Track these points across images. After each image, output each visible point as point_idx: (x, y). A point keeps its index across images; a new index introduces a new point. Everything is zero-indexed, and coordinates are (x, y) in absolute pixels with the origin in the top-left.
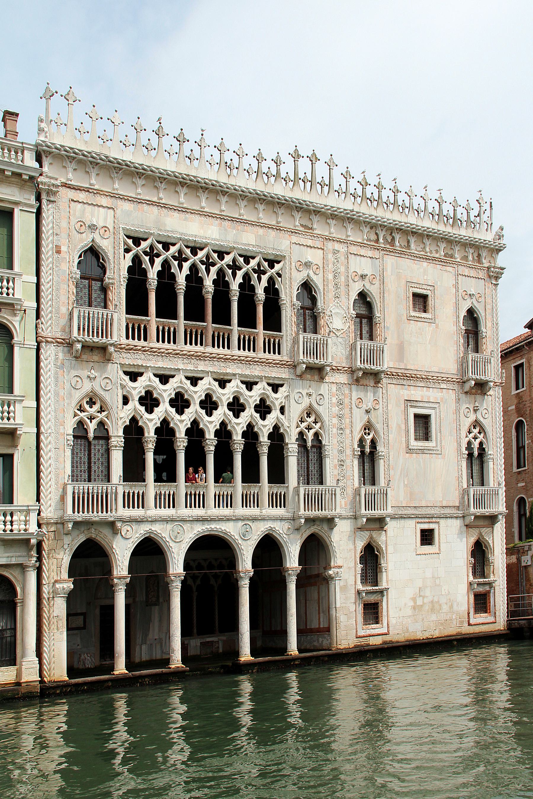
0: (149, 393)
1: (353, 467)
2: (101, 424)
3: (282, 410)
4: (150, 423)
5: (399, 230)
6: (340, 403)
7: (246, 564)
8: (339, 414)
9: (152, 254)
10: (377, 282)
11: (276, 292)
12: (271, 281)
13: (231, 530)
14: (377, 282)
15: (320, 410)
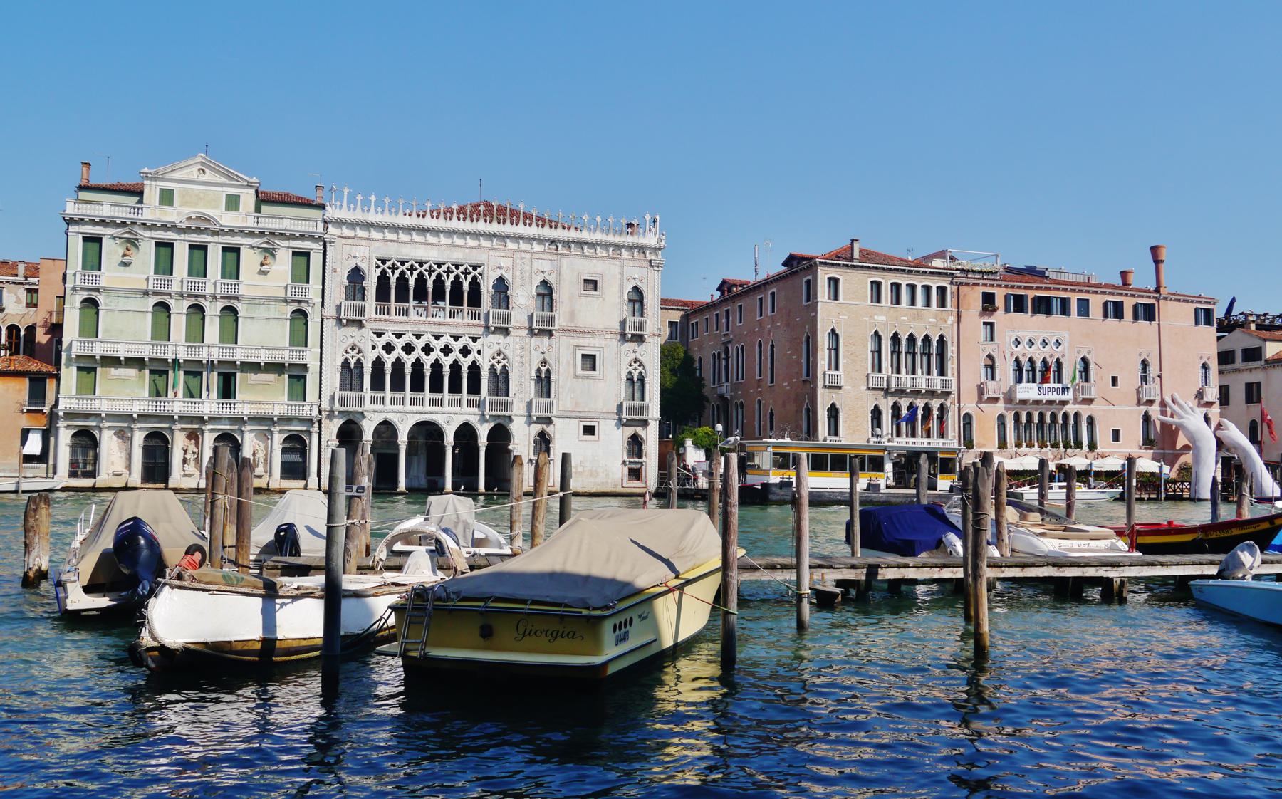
0: (388, 344)
1: (531, 388)
2: (359, 360)
3: (479, 352)
4: (389, 360)
5: (573, 242)
6: (522, 348)
7: (449, 440)
8: (520, 355)
9: (393, 268)
10: (554, 275)
11: (479, 285)
12: (475, 278)
13: (439, 419)
14: (554, 275)
15: (506, 352)
